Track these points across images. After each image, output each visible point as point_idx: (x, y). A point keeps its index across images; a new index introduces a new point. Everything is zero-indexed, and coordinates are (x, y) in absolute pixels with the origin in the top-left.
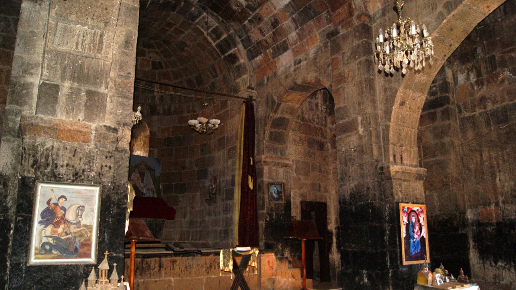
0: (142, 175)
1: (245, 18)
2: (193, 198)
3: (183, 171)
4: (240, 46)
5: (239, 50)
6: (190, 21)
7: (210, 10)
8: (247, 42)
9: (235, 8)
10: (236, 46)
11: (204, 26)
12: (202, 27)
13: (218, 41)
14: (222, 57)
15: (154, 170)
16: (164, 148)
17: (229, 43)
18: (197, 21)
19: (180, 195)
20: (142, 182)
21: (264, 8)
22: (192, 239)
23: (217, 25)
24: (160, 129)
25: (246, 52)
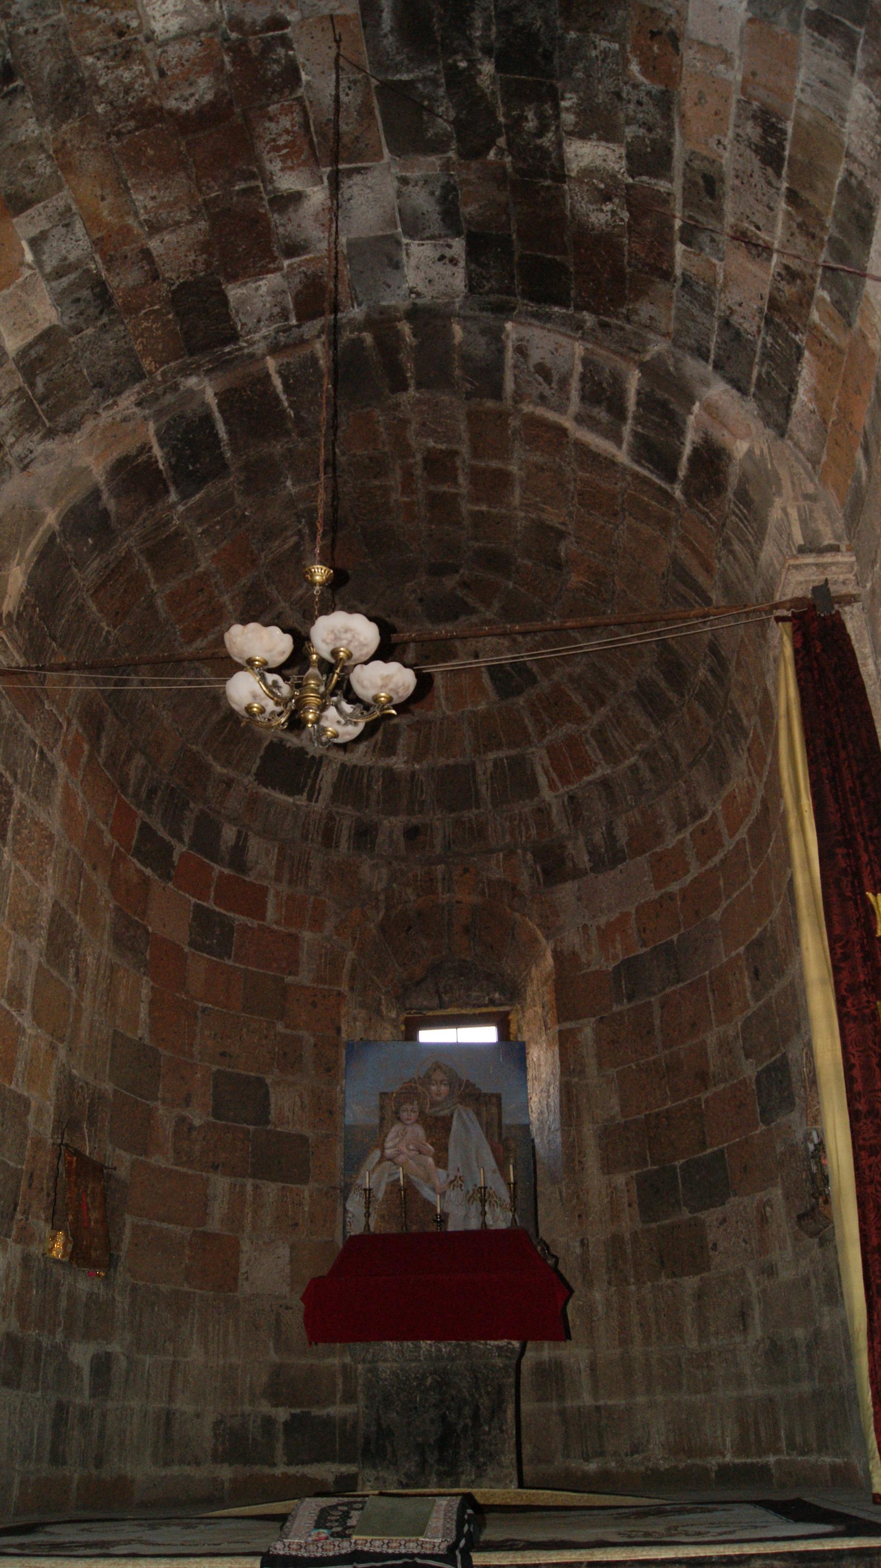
0: (438, 1129)
1: (662, 241)
2: (763, 1220)
3: (704, 1096)
4: (718, 391)
5: (710, 408)
6: (490, 404)
7: (533, 307)
8: (731, 358)
9: (599, 217)
10: (690, 399)
11: (545, 389)
12: (543, 398)
13: (627, 430)
14: (678, 494)
15: (498, 1097)
16: (616, 1008)
17: (665, 403)
18: (509, 386)
19: (712, 1216)
20: (441, 1162)
21: (689, 108)
22: (792, 1446)
23: (579, 349)
24: (593, 933)
25: (752, 405)
